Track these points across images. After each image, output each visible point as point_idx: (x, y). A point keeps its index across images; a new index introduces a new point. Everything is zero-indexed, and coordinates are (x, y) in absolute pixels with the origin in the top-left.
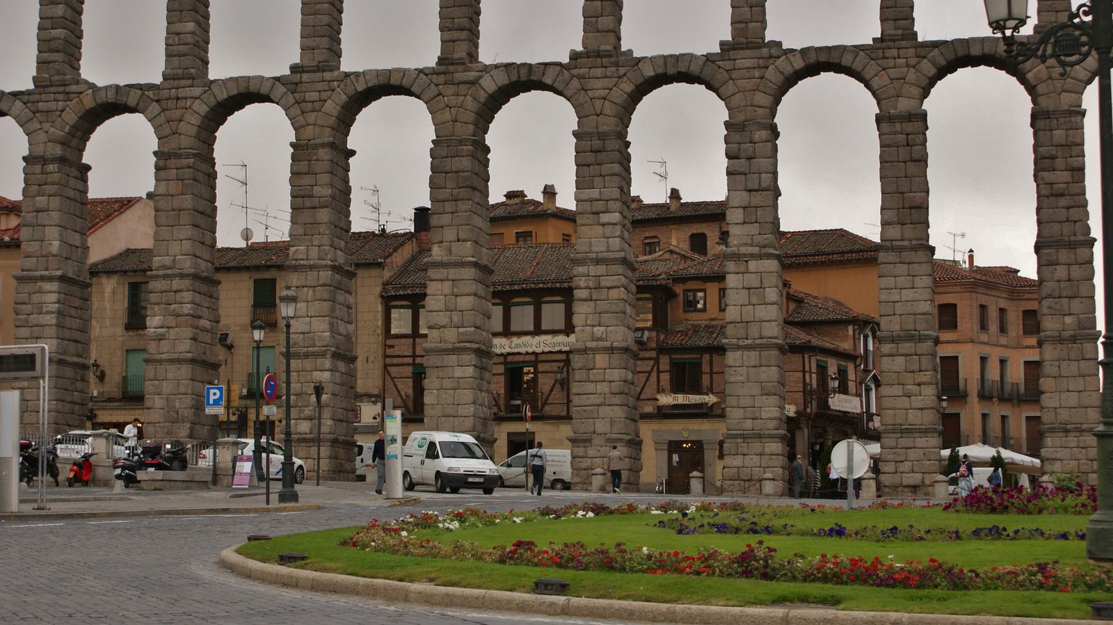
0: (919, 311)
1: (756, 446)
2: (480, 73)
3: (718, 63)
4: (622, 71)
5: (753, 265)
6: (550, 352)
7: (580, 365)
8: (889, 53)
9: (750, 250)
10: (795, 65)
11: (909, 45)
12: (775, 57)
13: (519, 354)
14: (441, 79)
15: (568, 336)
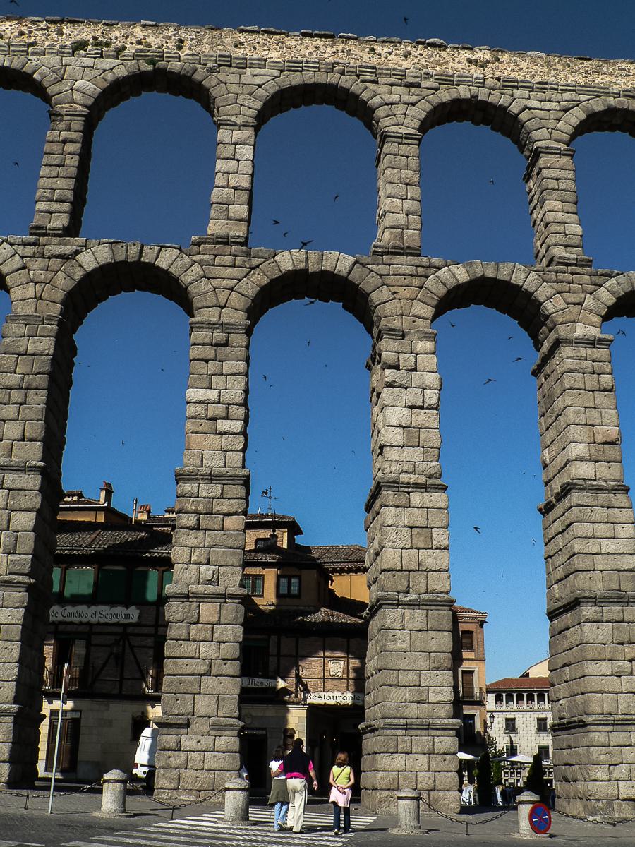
0: (624, 567)
1: (422, 740)
2: (79, 248)
3: (369, 266)
4: (255, 262)
5: (416, 497)
6: (106, 624)
7: (179, 616)
8: (561, 276)
9: (412, 478)
10: (459, 277)
11: (584, 271)
12: (435, 267)
13: (72, 623)
14: (29, 250)
15: (127, 608)
